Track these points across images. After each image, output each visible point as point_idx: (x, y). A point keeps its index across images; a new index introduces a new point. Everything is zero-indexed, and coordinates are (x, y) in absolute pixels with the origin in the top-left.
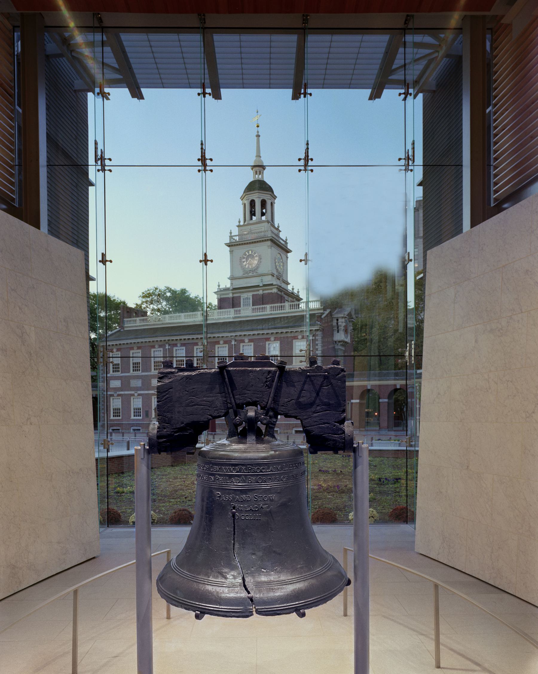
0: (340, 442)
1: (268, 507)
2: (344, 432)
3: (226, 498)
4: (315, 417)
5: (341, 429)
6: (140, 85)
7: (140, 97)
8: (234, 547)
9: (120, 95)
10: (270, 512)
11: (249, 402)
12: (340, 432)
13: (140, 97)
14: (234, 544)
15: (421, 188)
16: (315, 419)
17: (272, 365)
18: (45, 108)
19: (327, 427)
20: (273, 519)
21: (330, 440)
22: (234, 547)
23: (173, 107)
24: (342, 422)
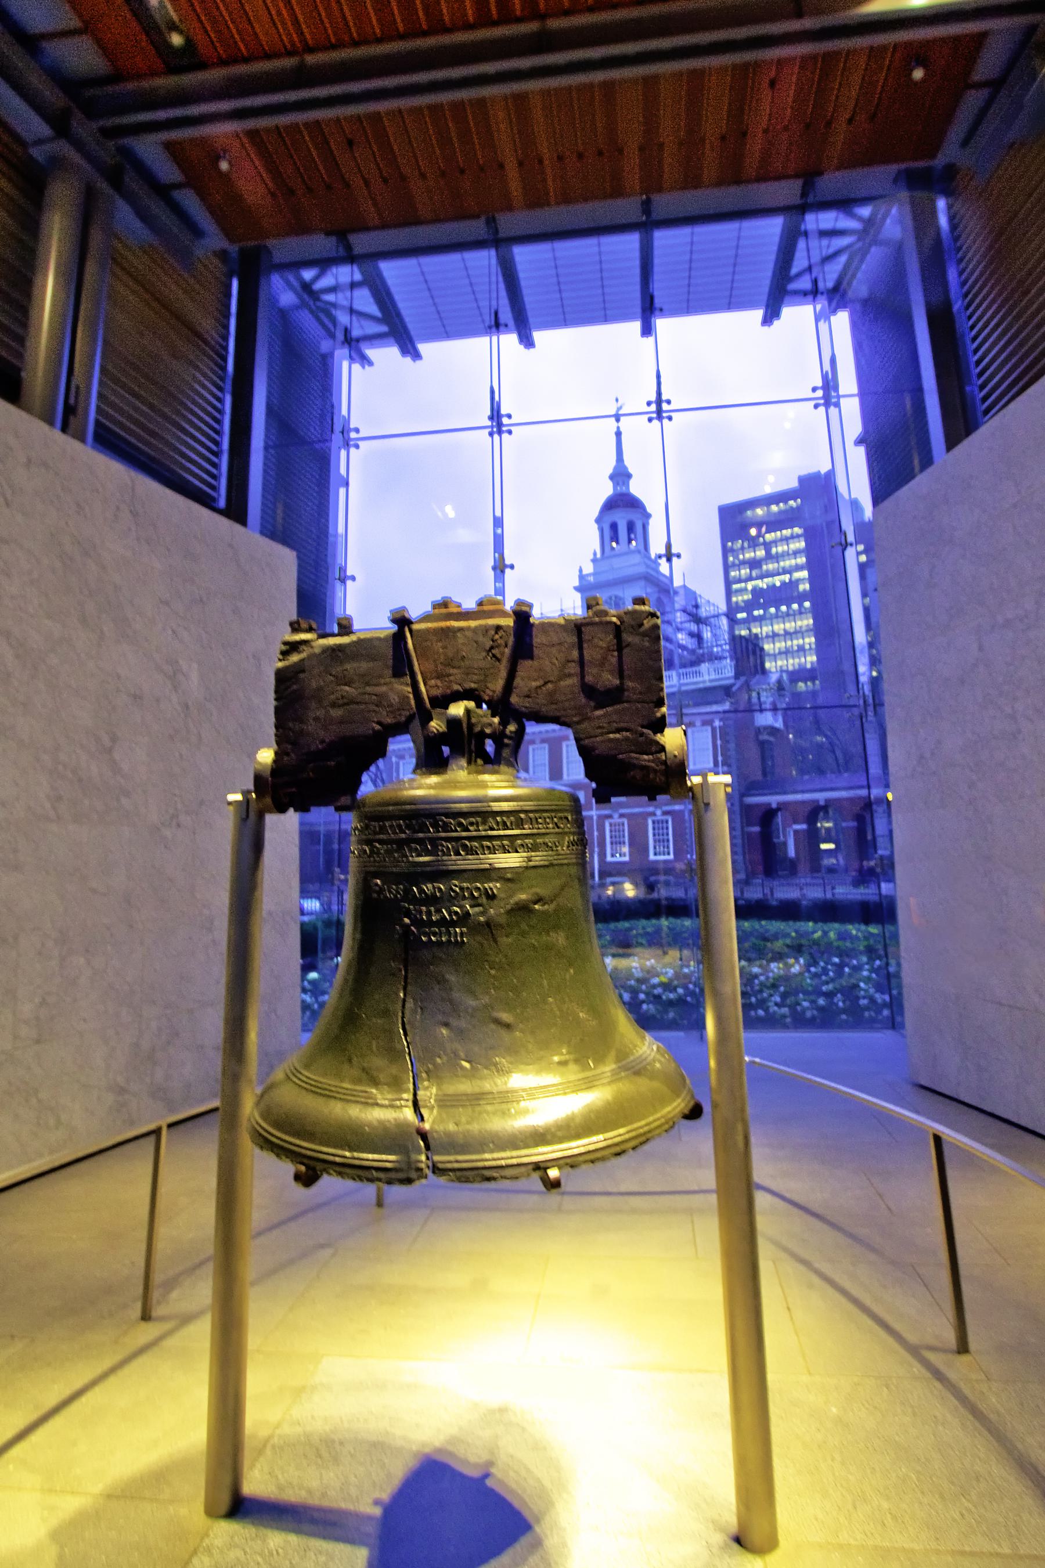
0: (655, 771)
1: (482, 913)
2: (663, 749)
3: (390, 892)
4: (599, 718)
5: (657, 743)
6: (415, 338)
7: (416, 356)
8: (403, 1006)
9: (386, 356)
10: (488, 924)
11: (458, 692)
12: (654, 749)
13: (416, 356)
14: (404, 1001)
15: (861, 450)
16: (596, 723)
17: (503, 614)
18: (265, 374)
19: (627, 739)
20: (495, 941)
21: (634, 766)
22: (403, 1006)
23: (462, 364)
24: (660, 726)
